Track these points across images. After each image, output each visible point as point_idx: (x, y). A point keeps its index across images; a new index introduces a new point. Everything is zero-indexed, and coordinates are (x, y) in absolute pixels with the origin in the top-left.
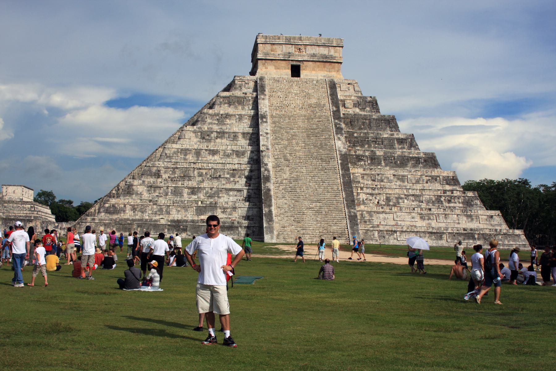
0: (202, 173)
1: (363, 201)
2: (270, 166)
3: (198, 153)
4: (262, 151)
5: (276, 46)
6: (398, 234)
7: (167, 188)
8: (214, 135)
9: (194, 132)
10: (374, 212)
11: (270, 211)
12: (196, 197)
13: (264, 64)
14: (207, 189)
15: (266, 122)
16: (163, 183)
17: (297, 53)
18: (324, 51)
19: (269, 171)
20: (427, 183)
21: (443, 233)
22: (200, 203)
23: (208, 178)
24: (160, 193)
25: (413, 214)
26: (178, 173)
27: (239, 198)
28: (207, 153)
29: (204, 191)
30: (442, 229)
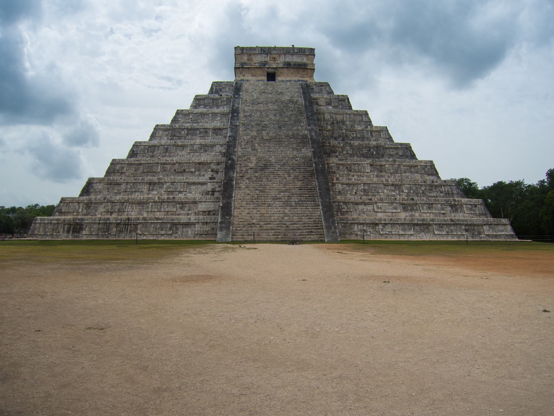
0: (167, 167)
1: (340, 192)
5: (253, 57)
6: (380, 227)
10: (352, 203)
12: (156, 193)
13: (241, 73)
14: (168, 184)
17: (272, 62)
18: (296, 59)
20: (405, 172)
21: (430, 225)
22: (156, 199)
25: (395, 204)
29: (165, 186)
30: (428, 220)
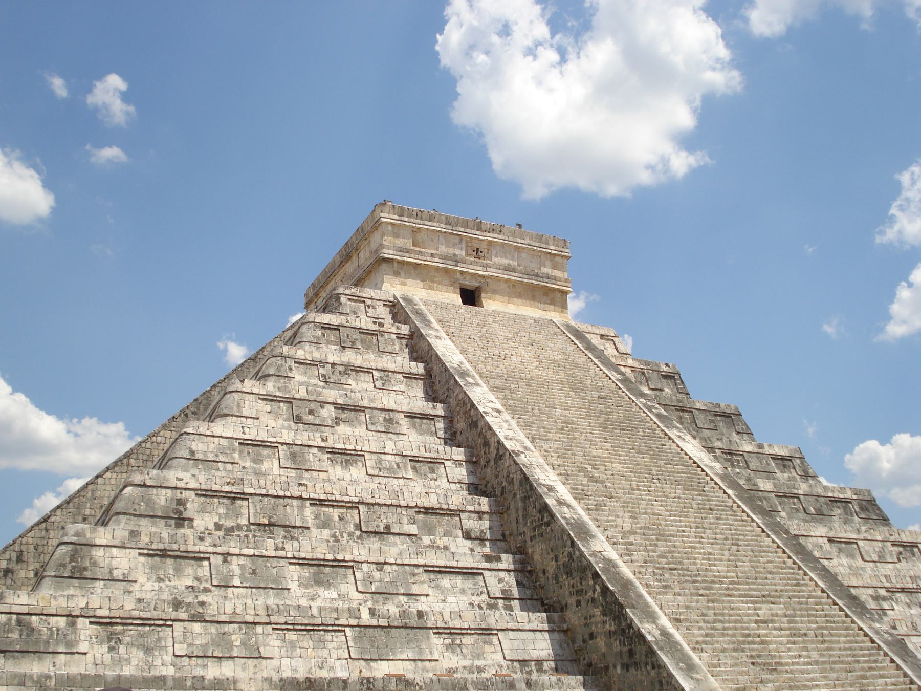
2: (563, 492)
3: (296, 455)
4: (518, 454)
7: (225, 561)
8: (328, 412)
9: (269, 399)
11: (664, 633)
12: (335, 595)
15: (477, 385)
16: (208, 540)
19: (569, 506)
23: (350, 535)
24: (198, 579)
26: (247, 512)
27: (475, 598)
28: (326, 456)
29: (359, 575)
